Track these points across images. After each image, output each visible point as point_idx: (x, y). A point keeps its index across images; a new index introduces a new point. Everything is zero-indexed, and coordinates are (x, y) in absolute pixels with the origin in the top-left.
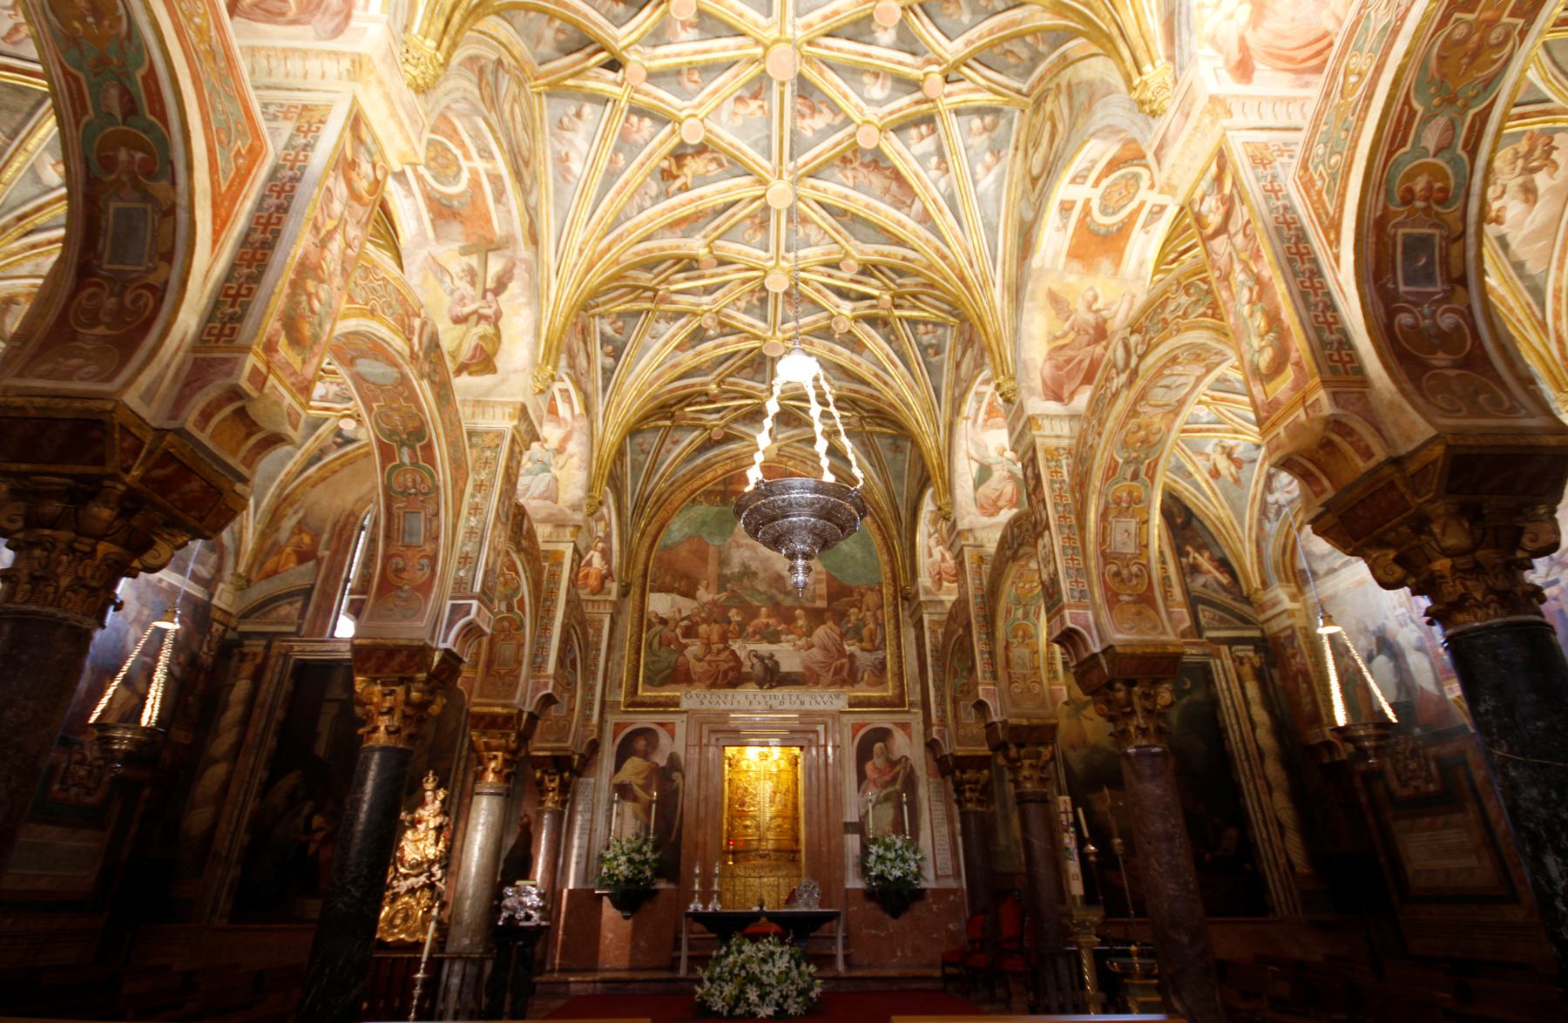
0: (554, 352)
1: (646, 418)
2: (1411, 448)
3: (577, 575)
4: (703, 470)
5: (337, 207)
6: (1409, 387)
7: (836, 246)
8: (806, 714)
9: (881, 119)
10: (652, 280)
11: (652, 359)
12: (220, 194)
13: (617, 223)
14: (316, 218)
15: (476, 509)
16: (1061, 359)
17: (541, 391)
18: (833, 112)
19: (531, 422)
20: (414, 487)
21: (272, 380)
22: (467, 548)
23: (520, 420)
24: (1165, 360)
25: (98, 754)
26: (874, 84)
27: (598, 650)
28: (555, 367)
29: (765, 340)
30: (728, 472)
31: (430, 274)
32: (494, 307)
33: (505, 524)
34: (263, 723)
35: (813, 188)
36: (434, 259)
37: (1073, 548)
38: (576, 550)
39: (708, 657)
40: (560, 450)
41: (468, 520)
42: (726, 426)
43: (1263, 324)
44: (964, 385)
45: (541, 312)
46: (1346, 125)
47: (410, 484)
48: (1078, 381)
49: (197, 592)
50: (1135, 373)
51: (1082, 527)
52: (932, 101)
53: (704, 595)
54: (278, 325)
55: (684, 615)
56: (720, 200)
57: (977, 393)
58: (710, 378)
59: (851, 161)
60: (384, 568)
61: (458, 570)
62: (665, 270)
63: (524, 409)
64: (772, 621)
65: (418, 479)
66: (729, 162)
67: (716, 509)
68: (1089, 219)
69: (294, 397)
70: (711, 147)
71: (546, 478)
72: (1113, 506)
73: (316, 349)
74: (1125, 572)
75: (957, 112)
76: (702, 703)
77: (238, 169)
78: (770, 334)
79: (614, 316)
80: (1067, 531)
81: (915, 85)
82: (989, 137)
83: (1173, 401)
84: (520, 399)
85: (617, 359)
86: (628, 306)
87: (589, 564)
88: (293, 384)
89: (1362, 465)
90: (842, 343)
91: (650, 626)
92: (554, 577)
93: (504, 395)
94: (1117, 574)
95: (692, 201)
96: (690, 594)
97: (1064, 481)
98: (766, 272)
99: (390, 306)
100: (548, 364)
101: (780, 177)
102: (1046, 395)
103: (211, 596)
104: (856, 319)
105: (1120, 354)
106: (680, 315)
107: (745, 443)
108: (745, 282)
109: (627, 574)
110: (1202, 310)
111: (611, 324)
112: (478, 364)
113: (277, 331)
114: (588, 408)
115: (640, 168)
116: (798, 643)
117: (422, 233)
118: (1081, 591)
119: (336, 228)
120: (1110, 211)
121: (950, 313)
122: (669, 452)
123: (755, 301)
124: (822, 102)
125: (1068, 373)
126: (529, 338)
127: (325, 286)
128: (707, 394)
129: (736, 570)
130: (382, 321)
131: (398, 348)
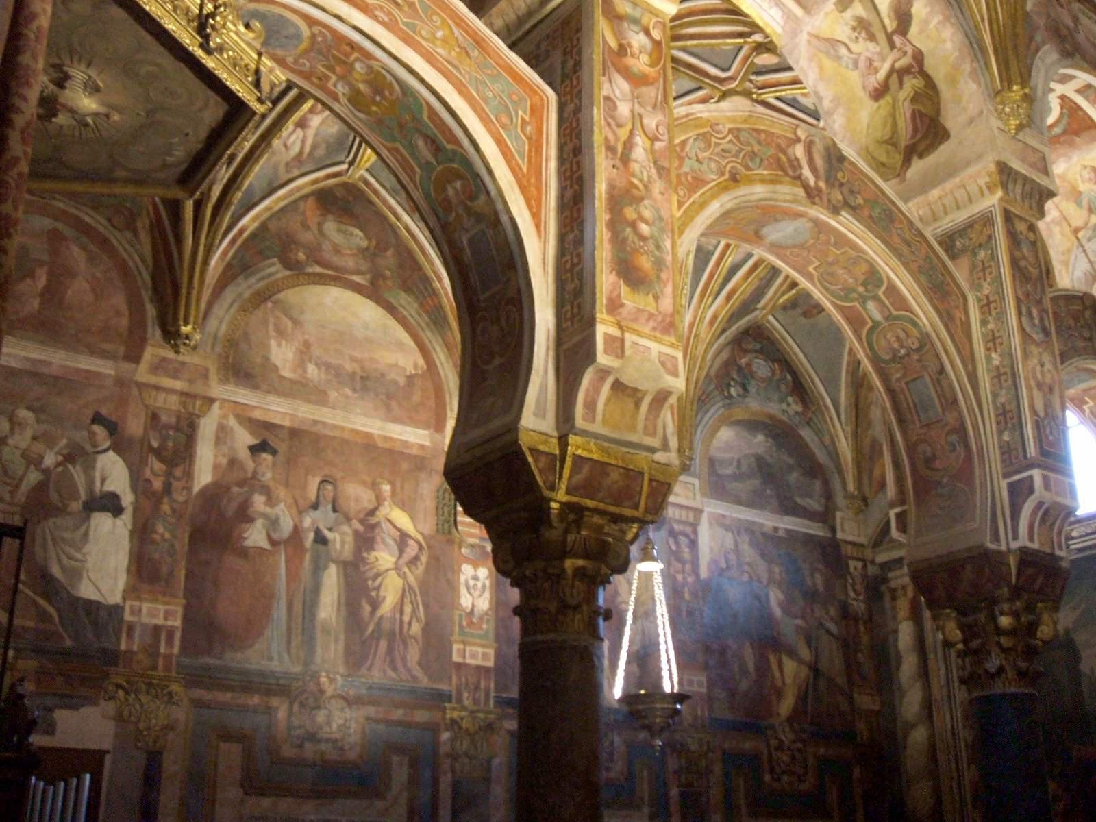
5: (624, 109)
12: (524, 176)
14: (606, 139)
15: (994, 339)
17: (1020, 127)
19: (1026, 179)
20: (902, 347)
21: (629, 338)
22: (1002, 400)
23: (1004, 186)
25: (791, 736)
31: (821, 55)
32: (909, 49)
33: (1046, 344)
34: (943, 672)
36: (817, 37)
41: (989, 358)
47: (896, 345)
49: (817, 530)
54: (613, 278)
60: (912, 464)
61: (1000, 433)
65: (902, 335)
69: (660, 342)
73: (664, 276)
77: (529, 139)
88: (654, 329)
99: (753, 155)
103: (833, 530)
112: (925, 137)
113: (615, 287)
117: (789, 16)
119: (631, 132)
127: (646, 202)
130: (750, 181)
131: (788, 197)
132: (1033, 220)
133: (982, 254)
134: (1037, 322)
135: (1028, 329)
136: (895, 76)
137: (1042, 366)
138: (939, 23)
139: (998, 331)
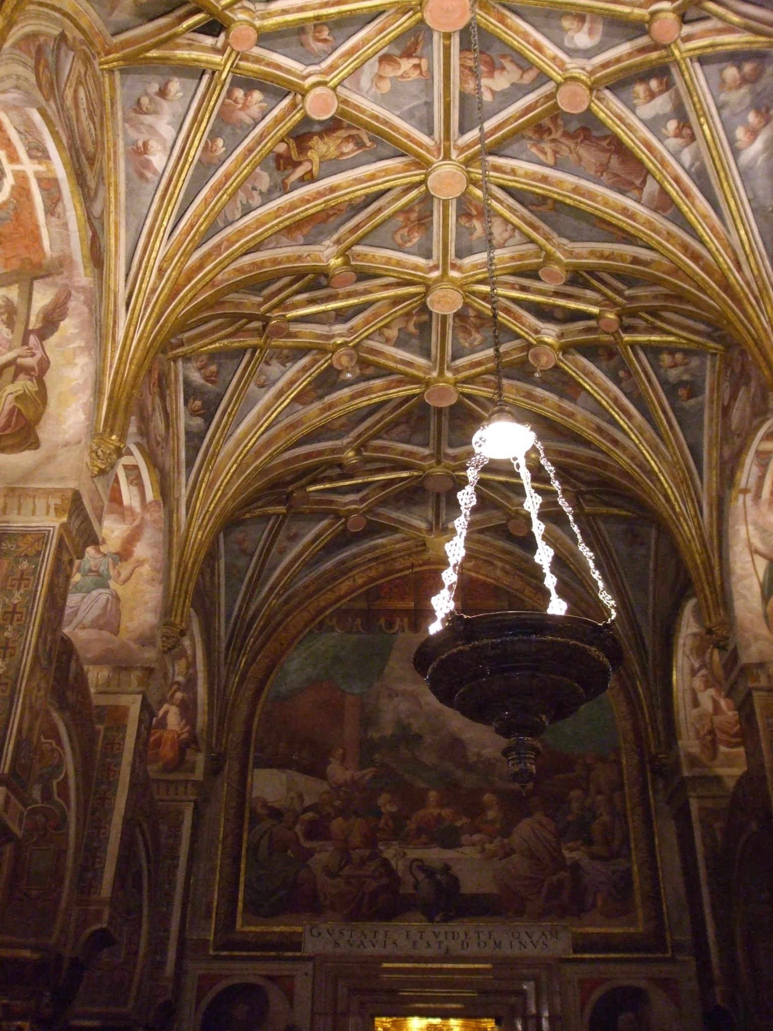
0: (121, 415)
1: (249, 502)
3: (146, 744)
4: (335, 579)
7: (531, 246)
8: (503, 964)
9: (591, 73)
10: (261, 305)
11: (260, 417)
13: (213, 229)
17: (102, 472)
18: (520, 67)
19: (86, 517)
23: (70, 517)
26: (579, 30)
27: (176, 858)
28: (123, 437)
29: (428, 384)
30: (373, 580)
32: (39, 354)
35: (496, 169)
38: (146, 706)
39: (347, 871)
40: (124, 554)
42: (369, 511)
45: (104, 360)
52: (666, 47)
53: (338, 772)
55: (307, 803)
56: (360, 191)
58: (346, 441)
59: (549, 131)
62: (280, 290)
63: (77, 497)
64: (446, 812)
66: (371, 139)
67: (354, 638)
70: (346, 122)
71: (101, 596)
75: (703, 60)
76: (337, 944)
78: (435, 374)
79: (204, 357)
81: (638, 28)
82: (751, 92)
84: (72, 485)
85: (208, 419)
86: (226, 342)
87: (163, 723)
90: (544, 384)
91: (255, 819)
92: (113, 747)
93: (49, 480)
95: (320, 194)
96: (316, 770)
98: (428, 287)
100: (112, 432)
101: (447, 157)
104: (565, 349)
106: (301, 352)
107: (398, 536)
108: (396, 301)
109: (219, 741)
111: (200, 369)
114: (165, 491)
115: (246, 157)
116: (487, 846)
122: (283, 552)
123: (412, 328)
124: (504, 56)
126: (85, 397)
128: (340, 466)
129: (388, 731)
132: (75, 557)
133: (25, 565)
134: (48, 647)
135: (40, 652)
136: (12, 369)
137: (39, 691)
138: (78, 347)
139: (14, 641)
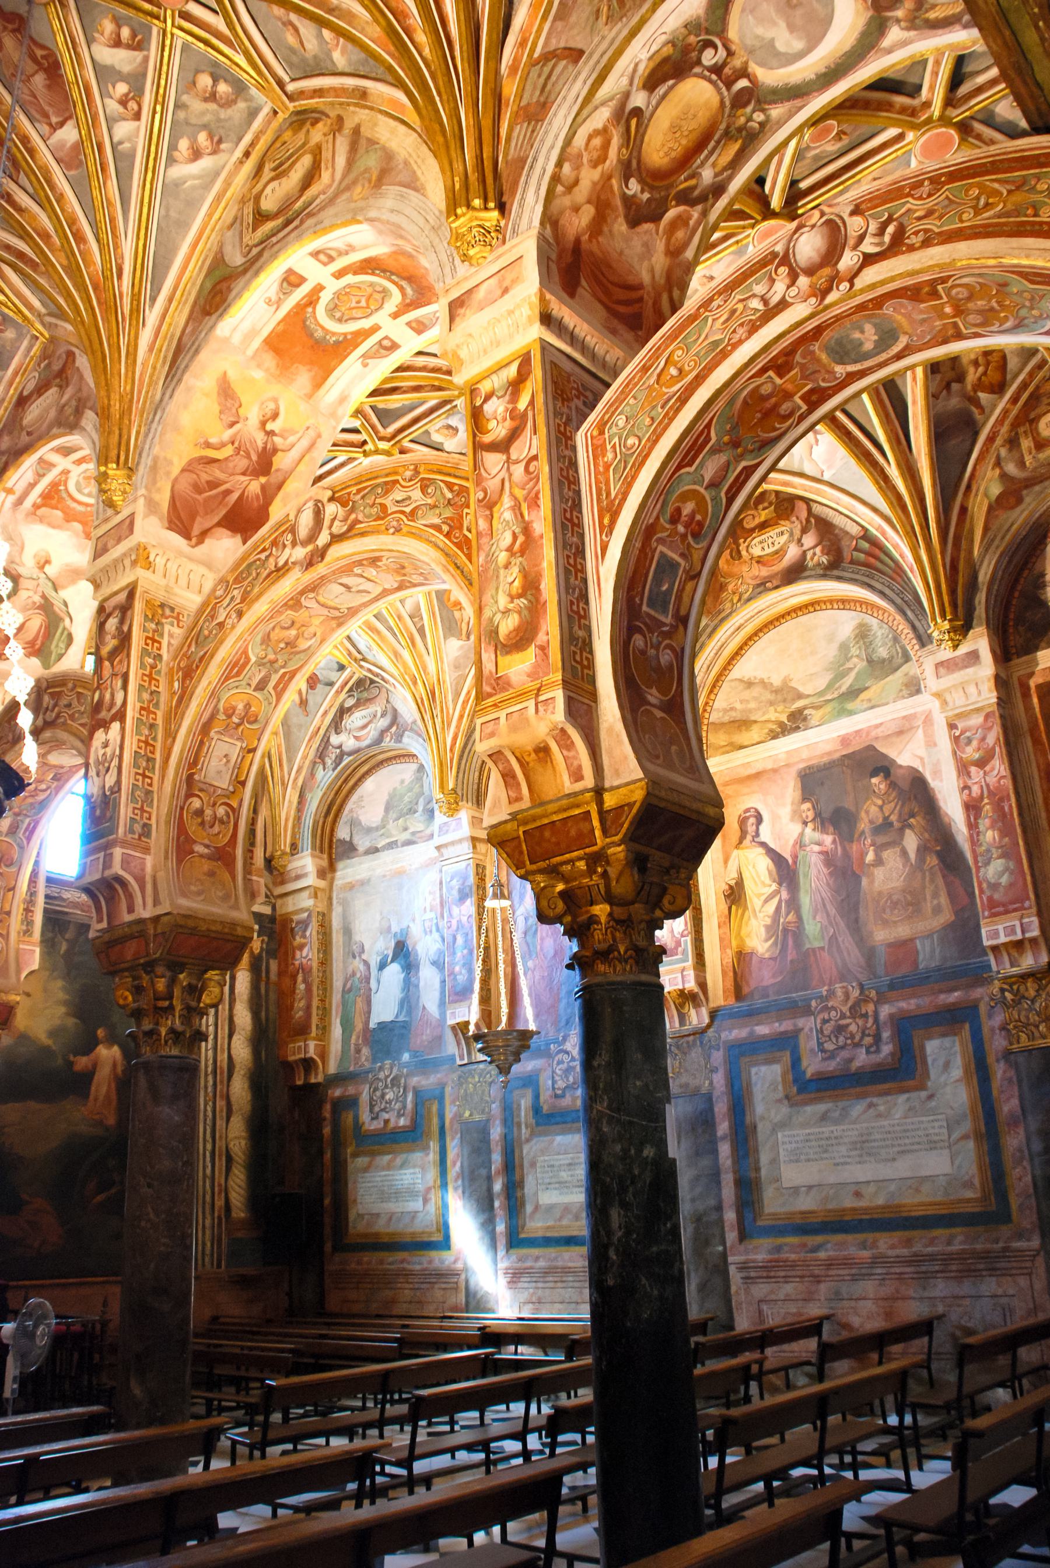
2: (616, 783)
6: (629, 716)
16: (205, 477)
24: (366, 556)
37: (149, 760)
43: (516, 583)
44: (25, 439)
46: (653, 413)
48: (216, 519)
50: (322, 553)
51: (171, 735)
57: (41, 460)
68: (310, 310)
72: (222, 717)
74: (208, 812)
80: (147, 732)
83: (344, 608)
89: (568, 786)
94: (200, 813)
97: (160, 656)
102: (170, 522)
105: (306, 520)
110: (437, 521)
118: (145, 825)
120: (338, 315)
121: (39, 316)
125: (206, 500)
